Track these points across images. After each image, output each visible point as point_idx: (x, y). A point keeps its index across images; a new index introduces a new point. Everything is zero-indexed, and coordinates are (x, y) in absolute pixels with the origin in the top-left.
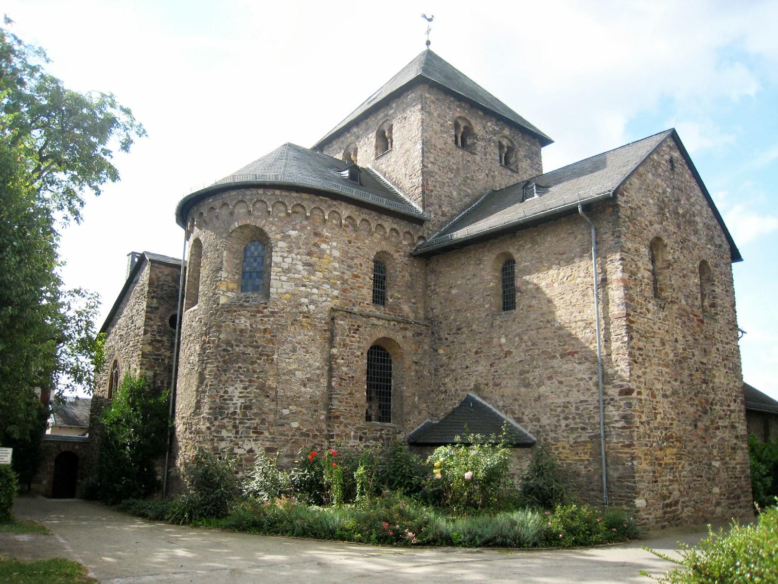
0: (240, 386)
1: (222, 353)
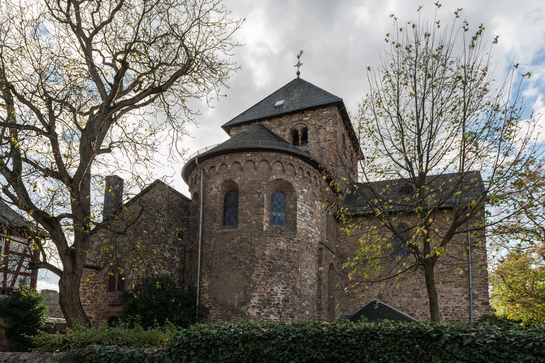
0: (282, 286)
1: (267, 264)
